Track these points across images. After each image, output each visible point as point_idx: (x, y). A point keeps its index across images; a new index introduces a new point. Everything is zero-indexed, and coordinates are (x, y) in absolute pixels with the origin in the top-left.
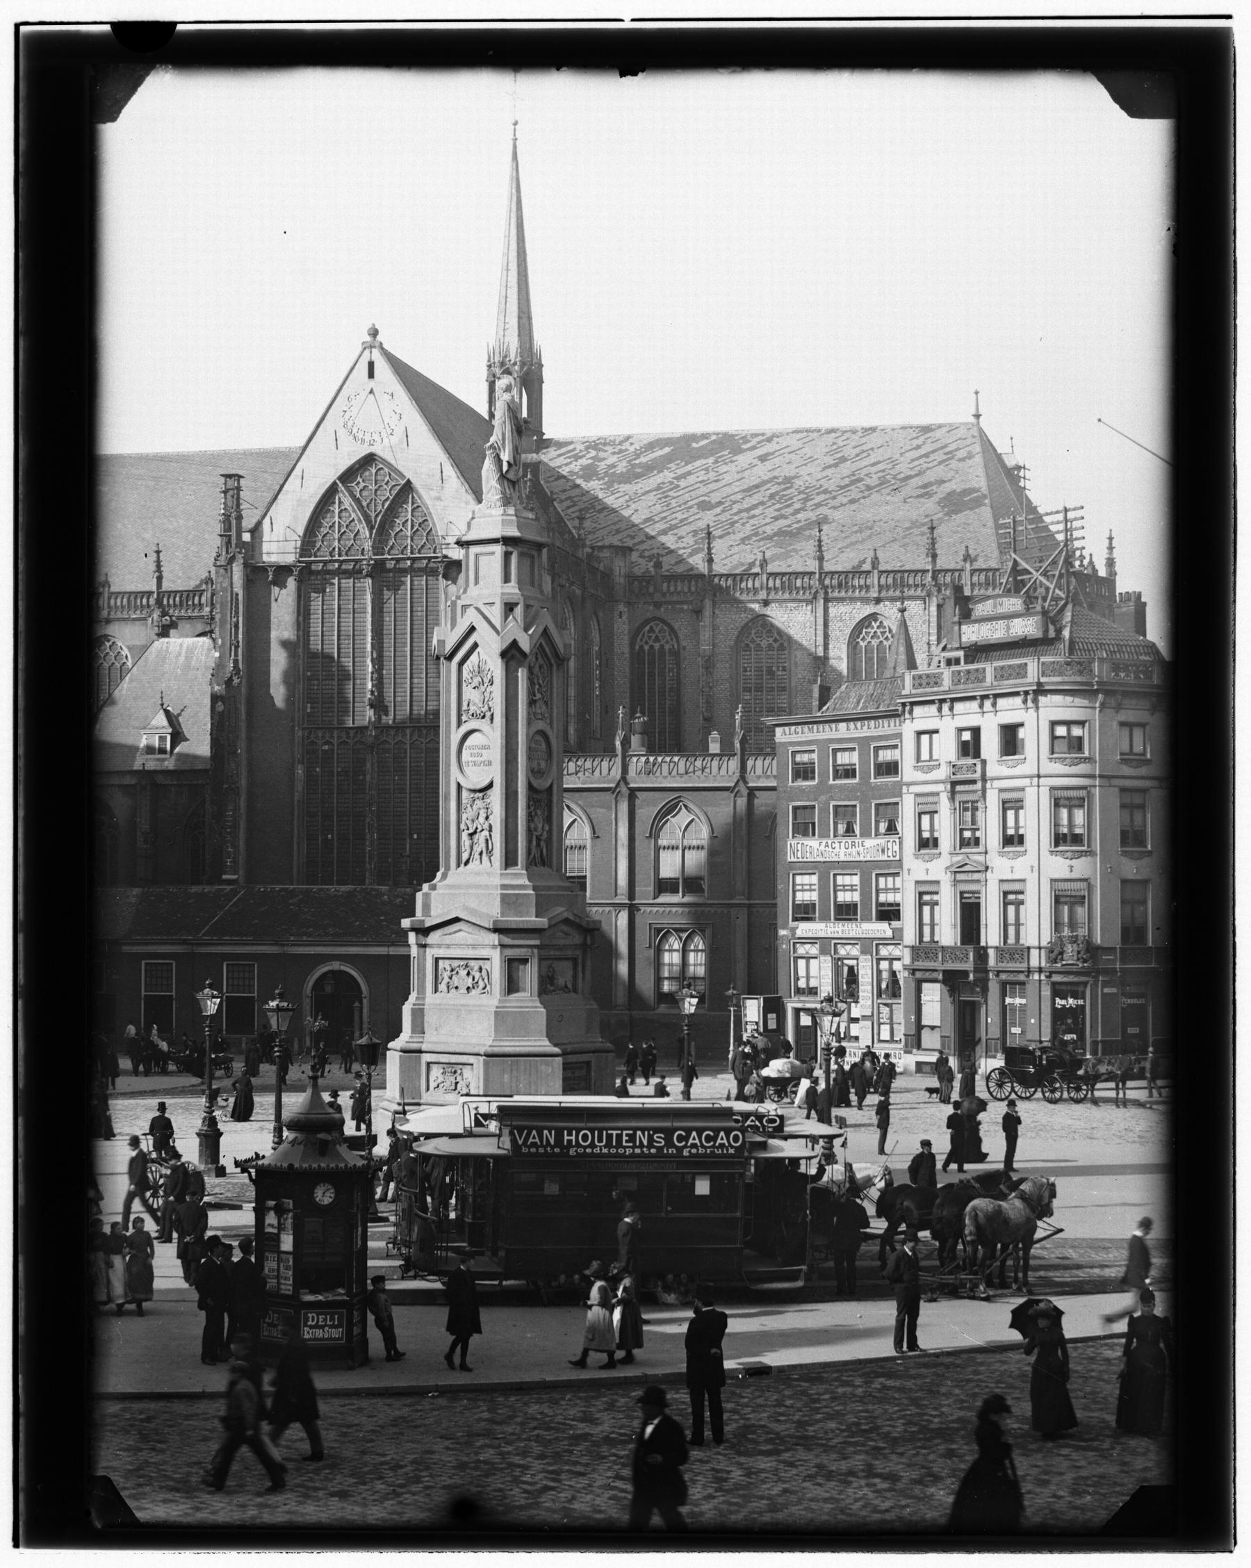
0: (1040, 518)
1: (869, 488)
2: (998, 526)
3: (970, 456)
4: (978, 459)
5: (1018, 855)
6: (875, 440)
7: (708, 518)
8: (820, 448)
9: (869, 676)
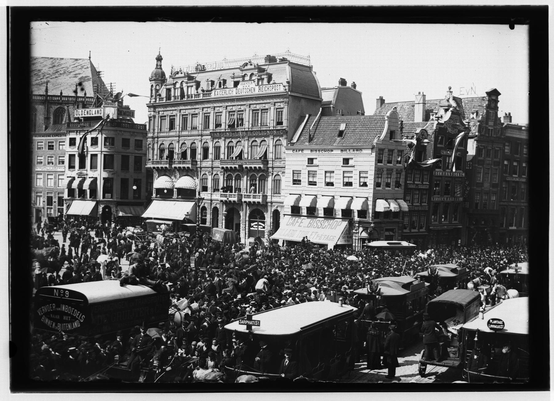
0: (104, 85)
1: (61, 74)
2: (93, 87)
3: (88, 68)
4: (90, 69)
5: (95, 171)
6: (62, 62)
8: (49, 62)
9: (58, 123)
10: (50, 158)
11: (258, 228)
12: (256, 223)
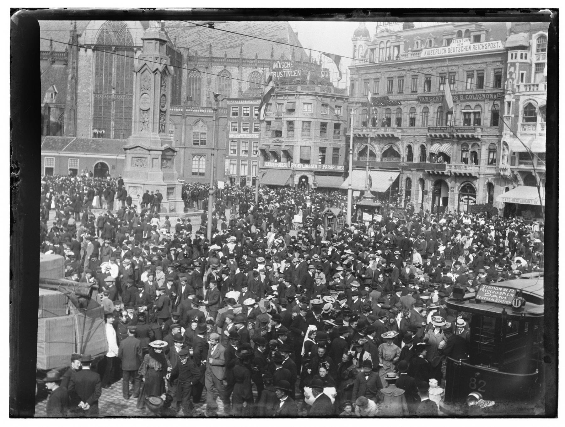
7: (211, 41)
10: (245, 125)
11: (468, 202)
12: (467, 197)
